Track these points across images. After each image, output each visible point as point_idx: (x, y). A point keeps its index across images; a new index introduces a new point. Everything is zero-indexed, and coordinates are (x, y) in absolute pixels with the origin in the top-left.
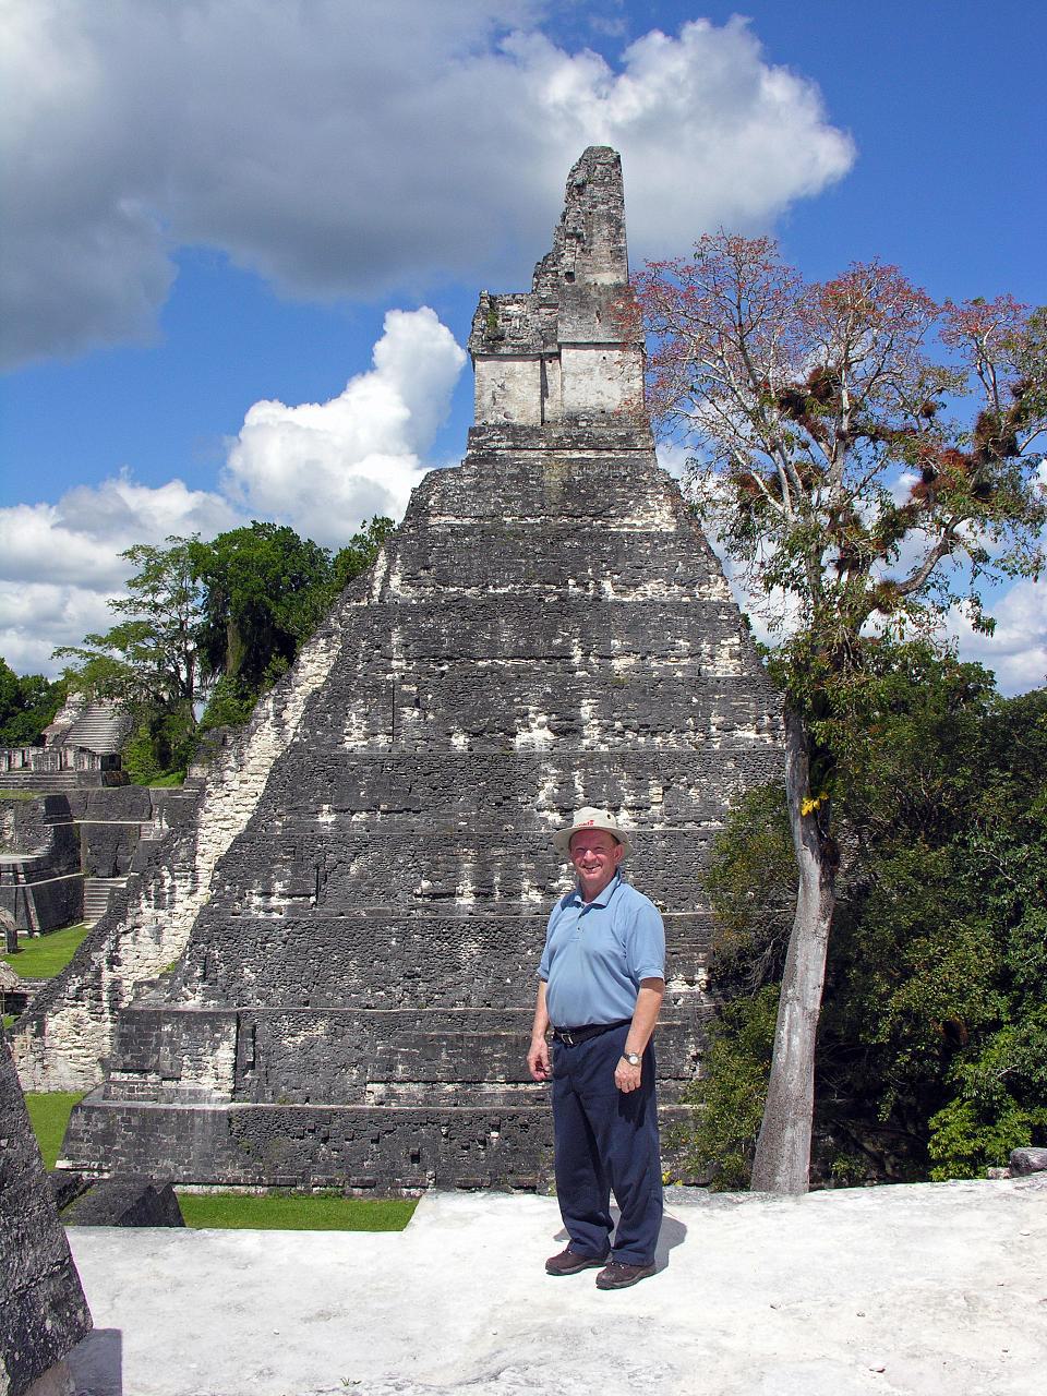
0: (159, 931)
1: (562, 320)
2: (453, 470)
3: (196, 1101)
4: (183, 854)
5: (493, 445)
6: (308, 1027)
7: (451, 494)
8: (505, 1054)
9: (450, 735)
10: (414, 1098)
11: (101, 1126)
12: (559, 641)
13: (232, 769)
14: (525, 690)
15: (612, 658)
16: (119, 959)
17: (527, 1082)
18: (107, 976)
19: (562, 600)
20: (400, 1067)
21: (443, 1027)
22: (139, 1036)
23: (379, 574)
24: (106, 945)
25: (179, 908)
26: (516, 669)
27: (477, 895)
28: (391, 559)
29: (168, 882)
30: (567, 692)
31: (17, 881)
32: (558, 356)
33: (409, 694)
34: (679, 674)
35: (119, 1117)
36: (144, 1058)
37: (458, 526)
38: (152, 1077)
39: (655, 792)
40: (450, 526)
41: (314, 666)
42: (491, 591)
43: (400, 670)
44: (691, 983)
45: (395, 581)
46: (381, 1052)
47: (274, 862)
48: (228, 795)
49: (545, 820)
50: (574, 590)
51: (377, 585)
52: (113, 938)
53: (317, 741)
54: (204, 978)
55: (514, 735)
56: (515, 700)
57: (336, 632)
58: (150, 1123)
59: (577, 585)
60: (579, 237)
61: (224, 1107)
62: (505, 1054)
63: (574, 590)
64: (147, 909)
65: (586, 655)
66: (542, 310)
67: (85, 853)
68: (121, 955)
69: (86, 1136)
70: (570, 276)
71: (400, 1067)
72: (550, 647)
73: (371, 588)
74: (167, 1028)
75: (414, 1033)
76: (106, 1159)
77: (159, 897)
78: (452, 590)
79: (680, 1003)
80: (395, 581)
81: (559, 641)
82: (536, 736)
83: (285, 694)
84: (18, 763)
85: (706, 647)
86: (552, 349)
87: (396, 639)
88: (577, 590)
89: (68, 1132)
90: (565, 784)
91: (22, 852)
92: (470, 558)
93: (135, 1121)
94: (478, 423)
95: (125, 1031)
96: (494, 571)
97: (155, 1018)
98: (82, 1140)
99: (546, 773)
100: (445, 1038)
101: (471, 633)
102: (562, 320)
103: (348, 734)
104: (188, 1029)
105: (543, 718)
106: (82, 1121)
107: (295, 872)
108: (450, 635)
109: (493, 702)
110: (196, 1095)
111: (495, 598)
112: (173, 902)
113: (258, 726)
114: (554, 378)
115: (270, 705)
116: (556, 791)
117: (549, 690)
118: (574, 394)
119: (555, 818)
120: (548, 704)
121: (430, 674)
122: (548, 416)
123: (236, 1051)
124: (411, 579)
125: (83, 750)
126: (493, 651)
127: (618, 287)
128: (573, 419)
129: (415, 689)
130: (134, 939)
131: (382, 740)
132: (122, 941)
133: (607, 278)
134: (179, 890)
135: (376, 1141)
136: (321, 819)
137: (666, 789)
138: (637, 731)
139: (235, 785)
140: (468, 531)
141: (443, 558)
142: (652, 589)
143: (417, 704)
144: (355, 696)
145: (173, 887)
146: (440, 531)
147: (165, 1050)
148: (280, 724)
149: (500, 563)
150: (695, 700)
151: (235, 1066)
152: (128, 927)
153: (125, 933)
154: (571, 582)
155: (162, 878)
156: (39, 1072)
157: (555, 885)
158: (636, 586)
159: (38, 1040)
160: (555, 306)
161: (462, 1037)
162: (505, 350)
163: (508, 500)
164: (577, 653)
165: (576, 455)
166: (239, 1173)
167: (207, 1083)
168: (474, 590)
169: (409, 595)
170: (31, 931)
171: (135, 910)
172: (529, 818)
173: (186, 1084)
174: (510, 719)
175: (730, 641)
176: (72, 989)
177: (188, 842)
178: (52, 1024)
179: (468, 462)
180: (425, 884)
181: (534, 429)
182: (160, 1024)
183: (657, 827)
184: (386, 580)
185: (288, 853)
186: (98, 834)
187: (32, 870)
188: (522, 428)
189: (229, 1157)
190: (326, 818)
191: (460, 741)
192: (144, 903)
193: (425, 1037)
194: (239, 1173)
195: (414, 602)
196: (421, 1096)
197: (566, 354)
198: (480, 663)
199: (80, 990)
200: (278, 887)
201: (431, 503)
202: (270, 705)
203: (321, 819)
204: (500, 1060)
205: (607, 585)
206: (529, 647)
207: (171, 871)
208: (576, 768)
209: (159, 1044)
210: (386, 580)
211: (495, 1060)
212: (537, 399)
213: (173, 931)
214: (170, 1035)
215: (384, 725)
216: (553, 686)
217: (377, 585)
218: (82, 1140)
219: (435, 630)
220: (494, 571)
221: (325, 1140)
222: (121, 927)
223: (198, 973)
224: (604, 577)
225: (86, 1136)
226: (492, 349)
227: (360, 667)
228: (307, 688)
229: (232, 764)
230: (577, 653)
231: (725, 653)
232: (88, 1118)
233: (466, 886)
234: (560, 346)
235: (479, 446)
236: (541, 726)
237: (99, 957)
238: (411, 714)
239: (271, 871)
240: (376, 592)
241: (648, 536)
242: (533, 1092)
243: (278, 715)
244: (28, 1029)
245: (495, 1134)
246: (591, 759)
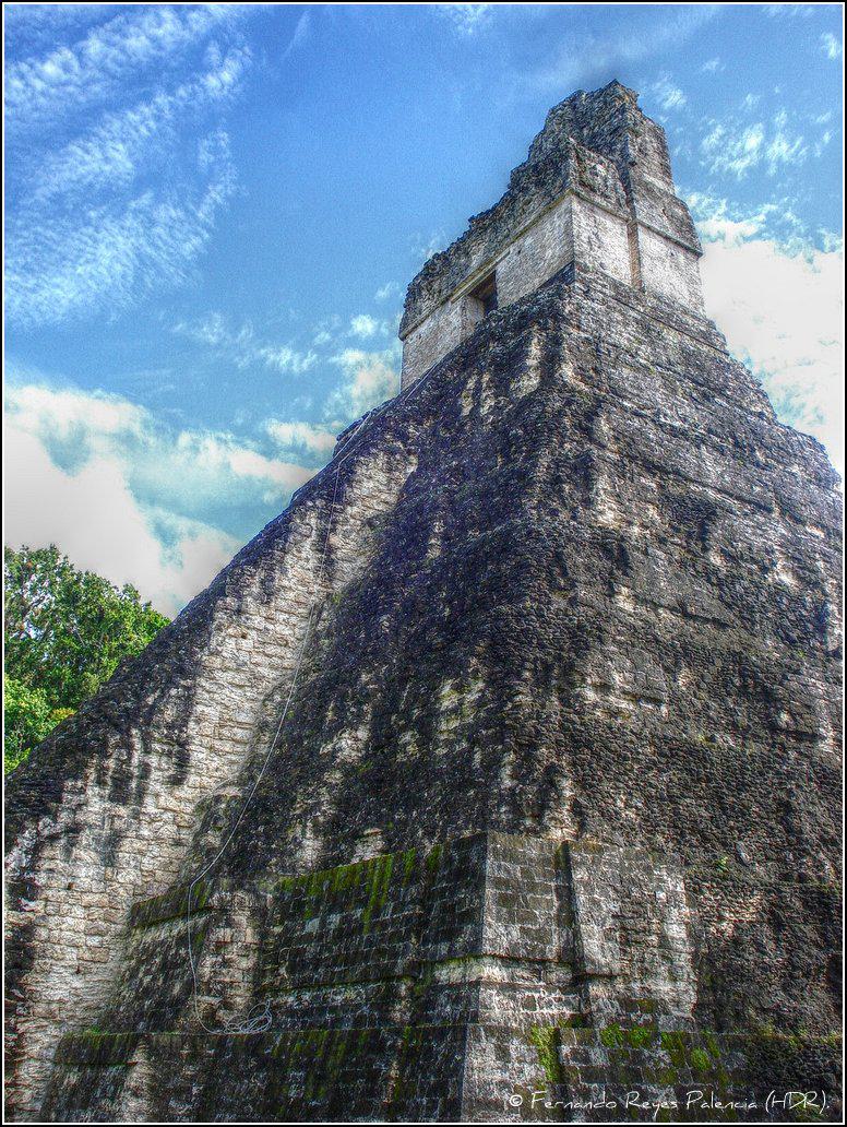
0: (115, 839)
4: (170, 714)
16: (34, 887)
48: (244, 637)
64: (96, 804)
68: (41, 879)
83: (335, 510)
112: (141, 793)
130: (68, 851)
134: (155, 775)
145: (145, 770)
148: (324, 547)
152: (59, 827)
153: (53, 838)
155: (130, 747)
171: (76, 799)
192: (93, 791)
207: (146, 739)
213: (138, 845)
229: (255, 589)
243: (323, 537)
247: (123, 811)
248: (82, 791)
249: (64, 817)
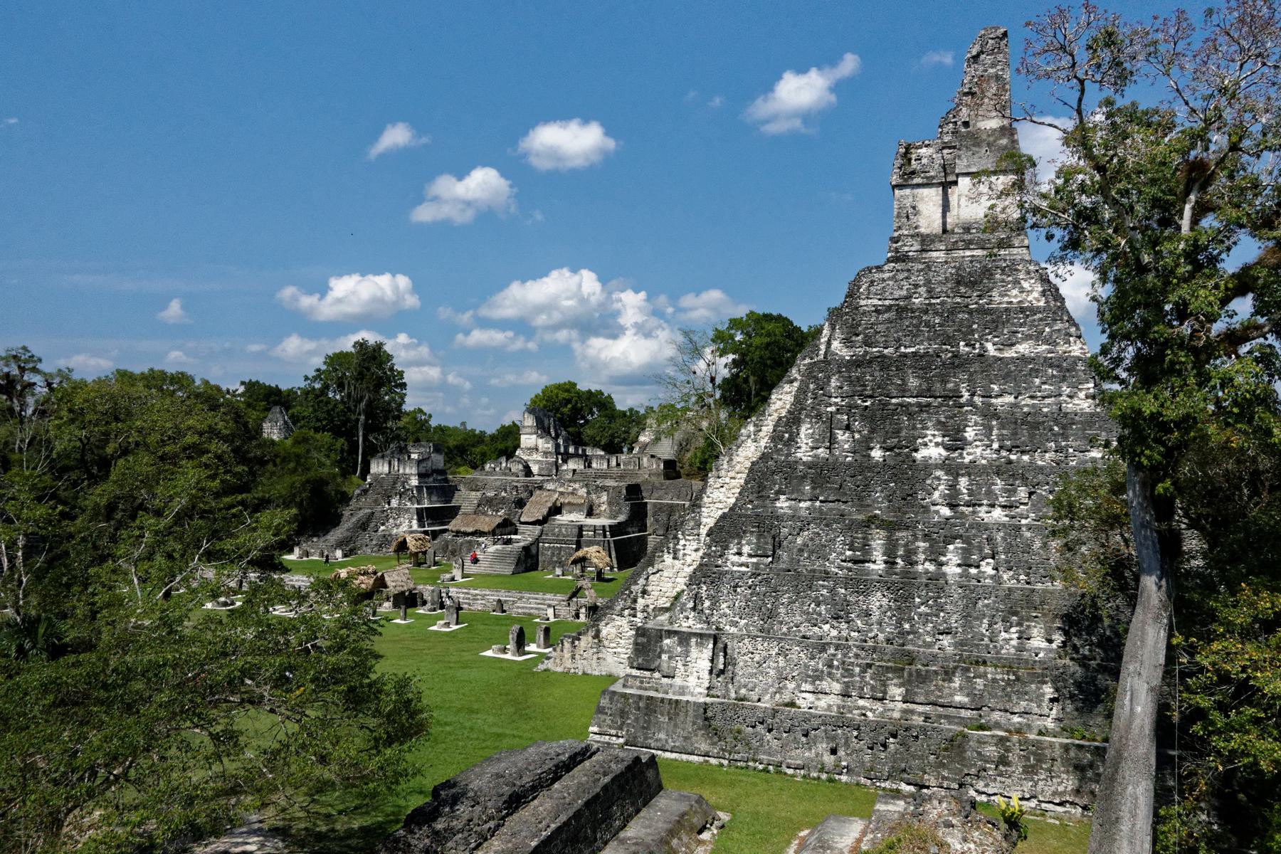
1: (959, 157)
2: (877, 267)
3: (683, 694)
5: (906, 249)
9: (872, 449)
15: (991, 397)
19: (955, 356)
22: (646, 647)
23: (824, 340)
24: (642, 581)
25: (689, 559)
26: (919, 405)
27: (886, 562)
28: (833, 328)
29: (682, 542)
31: (605, 536)
32: (955, 183)
34: (1045, 410)
38: (657, 675)
39: (1022, 493)
41: (782, 400)
42: (903, 349)
43: (836, 404)
44: (1050, 641)
45: (836, 345)
49: (937, 512)
50: (963, 348)
51: (823, 347)
53: (778, 451)
54: (694, 609)
57: (796, 379)
58: (650, 706)
59: (966, 345)
60: (973, 94)
61: (702, 700)
63: (963, 348)
64: (668, 558)
65: (973, 395)
66: (945, 151)
67: (650, 520)
68: (649, 588)
70: (966, 124)
73: (819, 350)
76: (621, 728)
77: (675, 552)
79: (1041, 655)
82: (932, 450)
84: (614, 463)
85: (1066, 390)
86: (951, 178)
87: (834, 382)
88: (967, 349)
89: (599, 706)
90: (953, 487)
94: (896, 234)
97: (661, 634)
102: (959, 157)
107: (758, 539)
110: (683, 690)
111: (905, 355)
114: (953, 200)
115: (751, 428)
118: (967, 210)
119: (946, 512)
121: (857, 407)
122: (949, 227)
123: (712, 661)
124: (847, 342)
125: (653, 456)
126: (903, 391)
127: (1003, 128)
128: (967, 229)
131: (822, 452)
133: (993, 123)
135: (806, 735)
136: (778, 505)
137: (1031, 494)
138: (1010, 451)
139: (727, 480)
140: (889, 308)
142: (1023, 348)
143: (848, 428)
147: (665, 657)
150: (1056, 428)
151: (711, 672)
154: (962, 343)
156: (594, 662)
157: (944, 559)
158: (1013, 345)
160: (954, 147)
162: (917, 180)
163: (916, 286)
164: (966, 395)
165: (968, 253)
167: (692, 681)
168: (891, 350)
169: (846, 354)
170: (612, 568)
172: (926, 509)
173: (678, 681)
175: (1086, 386)
176: (618, 608)
178: (604, 633)
179: (889, 261)
180: (849, 553)
181: (936, 236)
183: (1024, 522)
184: (829, 343)
186: (659, 509)
187: (616, 530)
188: (928, 235)
191: (877, 454)
192: (666, 556)
197: (960, 180)
198: (894, 401)
199: (623, 609)
200: (746, 549)
202: (751, 428)
203: (778, 505)
205: (989, 346)
206: (929, 390)
208: (963, 475)
210: (829, 343)
212: (939, 214)
217: (823, 347)
221: (770, 731)
222: (650, 570)
223: (691, 605)
224: (987, 340)
226: (906, 180)
228: (775, 416)
229: (725, 466)
230: (966, 395)
231: (1082, 395)
232: (611, 699)
233: (879, 556)
234: (958, 175)
235: (897, 251)
236: (937, 444)
238: (841, 436)
240: (822, 352)
241: (1022, 310)
245: (891, 740)
246: (971, 470)
247: (676, 562)
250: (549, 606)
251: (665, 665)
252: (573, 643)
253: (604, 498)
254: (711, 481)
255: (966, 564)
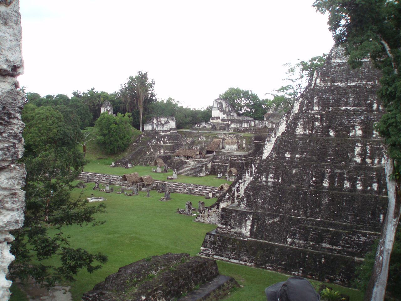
6: (273, 218)
7: (339, 52)
8: (330, 236)
10: (300, 245)
11: (213, 239)
12: (369, 101)
13: (273, 137)
14: (355, 118)
17: (337, 246)
18: (236, 194)
20: (297, 235)
21: (313, 225)
24: (236, 186)
26: (354, 111)
28: (318, 74)
30: (369, 119)
33: (317, 118)
35: (217, 238)
36: (227, 222)
37: (341, 63)
40: (338, 63)
43: (317, 110)
45: (318, 81)
46: (293, 230)
47: (270, 168)
52: (238, 184)
55: (349, 132)
56: (351, 121)
62: (330, 236)
69: (209, 242)
71: (297, 235)
72: (366, 103)
74: (233, 215)
75: (303, 225)
78: (336, 84)
80: (318, 81)
81: (369, 101)
87: (315, 100)
89: (205, 239)
90: (364, 150)
91: (247, 151)
92: (343, 74)
93: (221, 240)
95: (223, 214)
96: (350, 78)
98: (208, 242)
99: (357, 146)
100: (312, 228)
101: (340, 99)
103: (298, 130)
104: (239, 215)
105: (359, 127)
106: (208, 237)
107: (276, 171)
108: (333, 99)
109: (344, 122)
111: (350, 87)
113: (281, 124)
116: (360, 152)
117: (363, 118)
119: (358, 160)
120: (362, 123)
124: (324, 81)
126: (346, 104)
129: (319, 117)
132: (240, 185)
141: (334, 74)
144: (301, 119)
146: (335, 64)
149: (352, 75)
153: (242, 183)
159: (217, 210)
161: (316, 229)
164: (375, 106)
166: (247, 259)
171: (244, 177)
174: (349, 128)
177: (260, 158)
182: (232, 213)
185: (274, 166)
189: (245, 254)
190: (288, 155)
192: (247, 175)
193: (306, 227)
194: (247, 259)
195: (324, 88)
196: (302, 245)
199: (229, 197)
201: (332, 55)
202: (285, 118)
204: (328, 238)
208: (369, 145)
209: (231, 219)
211: (327, 237)
214: (234, 216)
215: (308, 128)
216: (365, 117)
218: (208, 242)
219: (328, 99)
220: (350, 78)
222: (240, 181)
225: (209, 242)
227: (304, 109)
232: (210, 237)
237: (235, 189)
239: (269, 171)
242: (338, 249)
244: (215, 207)
248: (245, 175)
249: (243, 179)
250: (210, 192)
251: (232, 225)
252: (208, 211)
253: (244, 142)
254: (266, 142)
255: (364, 185)
